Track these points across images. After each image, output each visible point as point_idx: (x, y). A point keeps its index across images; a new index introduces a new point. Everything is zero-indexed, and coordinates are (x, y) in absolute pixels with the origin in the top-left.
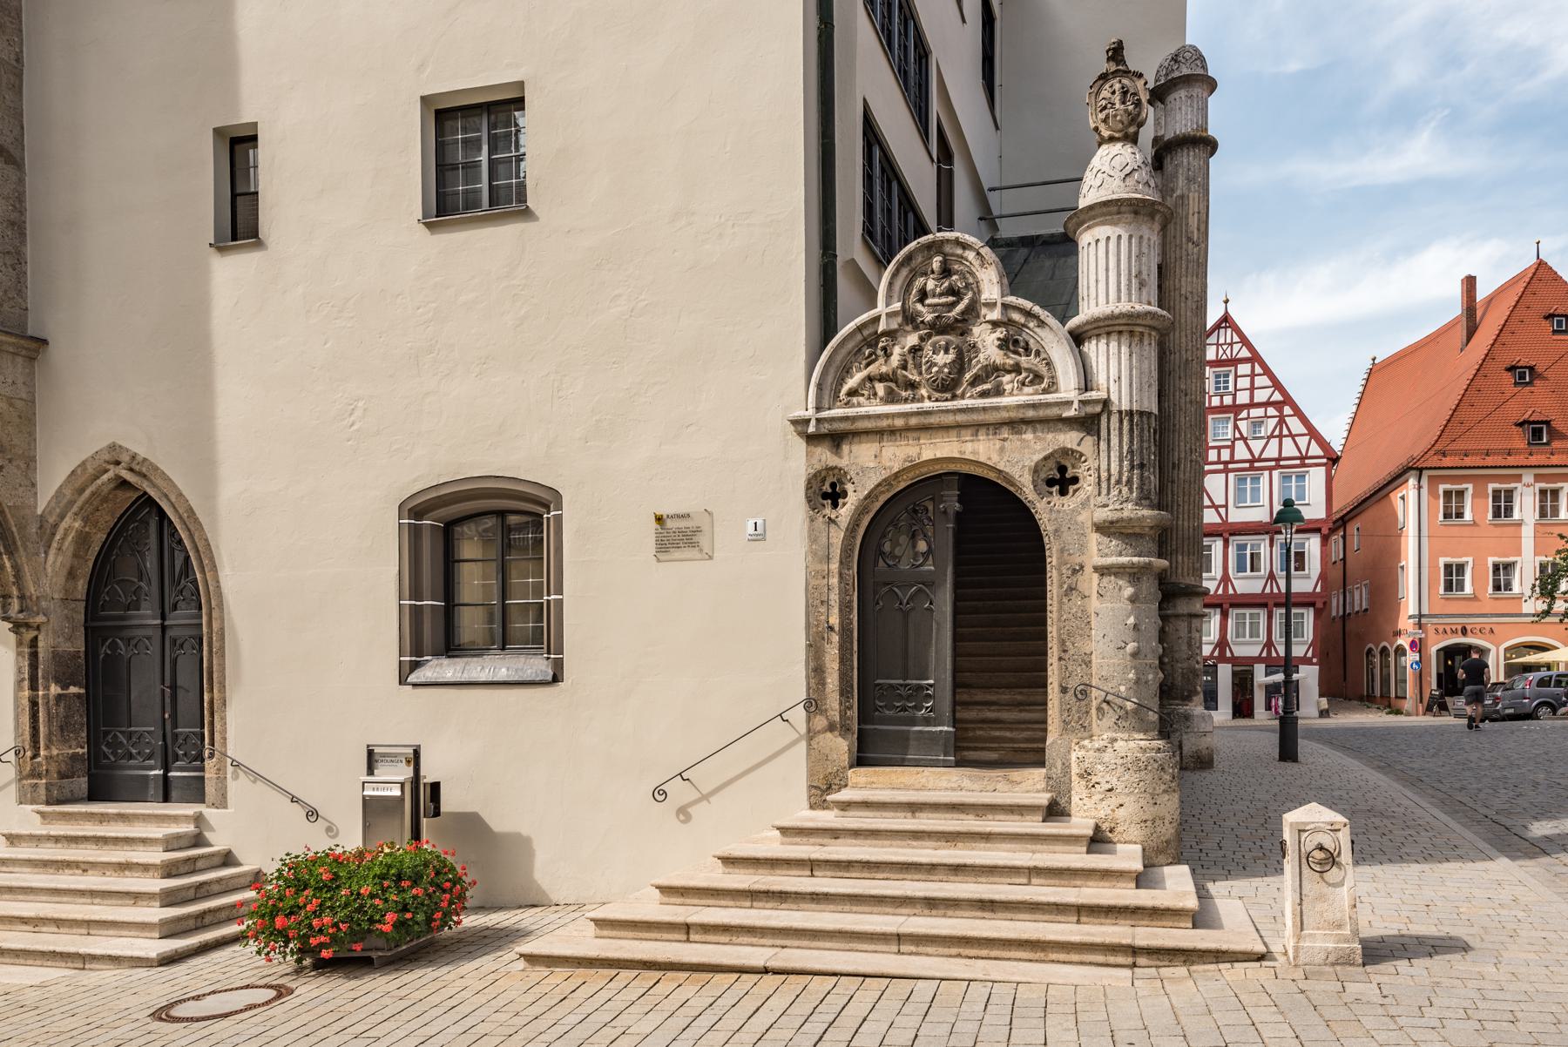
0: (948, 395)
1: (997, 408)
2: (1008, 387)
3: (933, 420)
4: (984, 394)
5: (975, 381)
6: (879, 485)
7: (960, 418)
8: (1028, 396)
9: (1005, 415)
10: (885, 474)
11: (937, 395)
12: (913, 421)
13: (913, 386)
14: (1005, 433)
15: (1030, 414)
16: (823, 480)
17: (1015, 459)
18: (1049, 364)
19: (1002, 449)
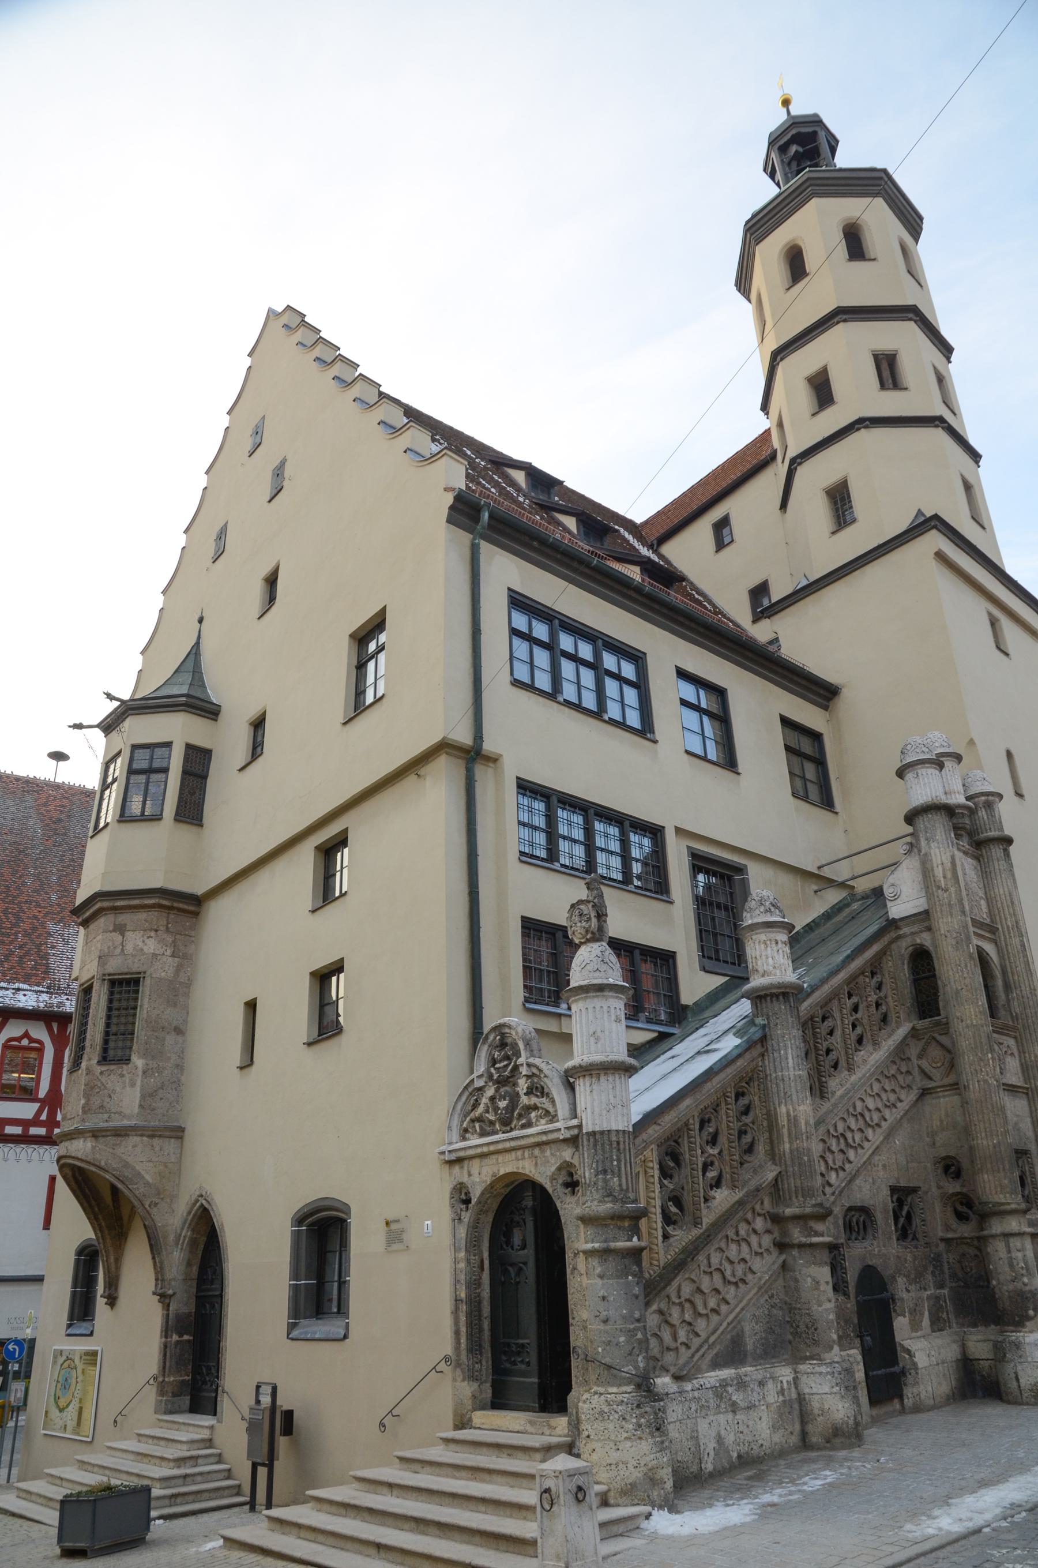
0: (508, 1128)
1: (528, 1136)
2: (534, 1121)
3: (500, 1146)
4: (523, 1127)
5: (520, 1116)
6: (482, 1194)
7: (513, 1144)
8: (542, 1126)
9: (532, 1140)
10: (484, 1186)
11: (504, 1129)
12: (492, 1148)
13: (492, 1123)
14: (537, 1151)
15: (544, 1138)
16: (461, 1193)
17: (542, 1170)
18: (553, 1102)
19: (536, 1164)
